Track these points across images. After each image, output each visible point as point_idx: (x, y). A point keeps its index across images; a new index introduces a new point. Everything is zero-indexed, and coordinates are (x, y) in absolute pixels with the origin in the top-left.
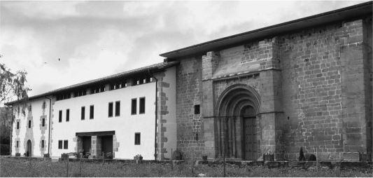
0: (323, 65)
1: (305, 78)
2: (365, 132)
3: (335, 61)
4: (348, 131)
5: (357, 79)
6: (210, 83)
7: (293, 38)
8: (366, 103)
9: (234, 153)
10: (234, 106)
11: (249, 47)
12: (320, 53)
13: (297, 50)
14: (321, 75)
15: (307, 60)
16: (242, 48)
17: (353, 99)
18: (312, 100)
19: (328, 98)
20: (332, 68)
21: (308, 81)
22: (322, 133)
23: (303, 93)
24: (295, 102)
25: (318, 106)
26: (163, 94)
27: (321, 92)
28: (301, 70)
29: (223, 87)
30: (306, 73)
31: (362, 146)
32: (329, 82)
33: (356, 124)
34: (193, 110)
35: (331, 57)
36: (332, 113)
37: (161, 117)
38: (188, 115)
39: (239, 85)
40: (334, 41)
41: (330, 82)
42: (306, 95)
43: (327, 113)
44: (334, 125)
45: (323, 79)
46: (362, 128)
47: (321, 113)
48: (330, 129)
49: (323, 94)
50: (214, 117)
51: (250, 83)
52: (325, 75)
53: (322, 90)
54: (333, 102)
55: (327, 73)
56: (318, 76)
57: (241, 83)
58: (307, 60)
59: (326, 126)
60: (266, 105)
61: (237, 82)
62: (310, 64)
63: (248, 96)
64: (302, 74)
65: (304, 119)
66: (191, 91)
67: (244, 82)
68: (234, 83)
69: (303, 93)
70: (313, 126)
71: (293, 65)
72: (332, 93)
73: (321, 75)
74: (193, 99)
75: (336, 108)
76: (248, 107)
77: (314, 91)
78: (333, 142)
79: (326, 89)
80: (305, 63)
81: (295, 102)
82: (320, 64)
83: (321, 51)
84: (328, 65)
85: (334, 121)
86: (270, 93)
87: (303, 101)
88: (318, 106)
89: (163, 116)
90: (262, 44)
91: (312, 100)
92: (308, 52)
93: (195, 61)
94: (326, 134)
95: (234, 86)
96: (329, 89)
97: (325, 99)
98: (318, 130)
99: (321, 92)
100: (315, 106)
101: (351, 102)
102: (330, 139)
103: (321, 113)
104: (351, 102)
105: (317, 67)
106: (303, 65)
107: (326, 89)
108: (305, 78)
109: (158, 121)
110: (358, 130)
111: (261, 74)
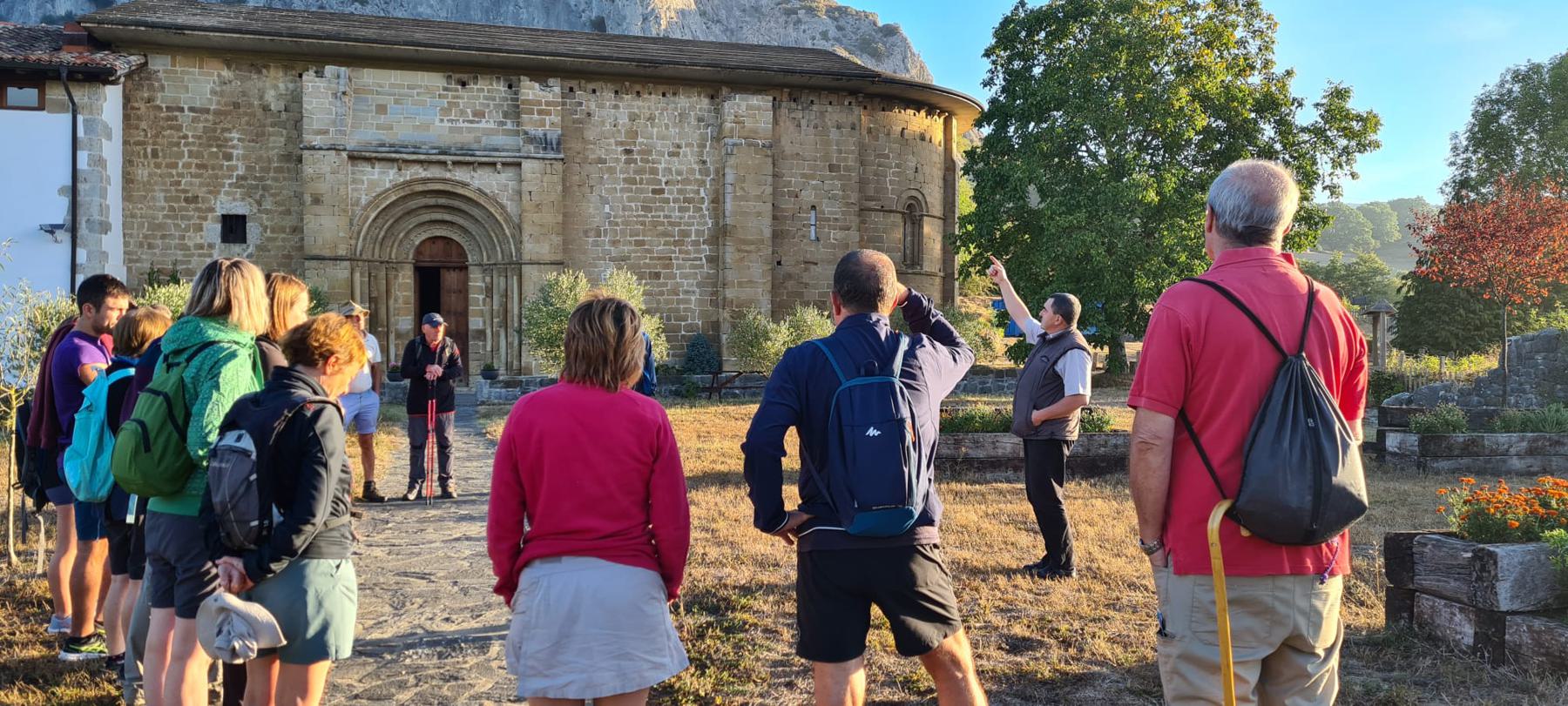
3: (696, 167)
5: (759, 214)
7: (594, 91)
11: (464, 84)
12: (660, 143)
13: (603, 123)
14: (662, 191)
15: (628, 152)
16: (435, 80)
18: (640, 243)
19: (676, 243)
20: (686, 181)
21: (630, 200)
24: (596, 244)
28: (611, 171)
30: (625, 180)
32: (681, 209)
38: (191, 244)
39: (444, 181)
40: (694, 122)
44: (687, 301)
45: (667, 201)
47: (657, 276)
48: (677, 310)
49: (665, 234)
52: (671, 192)
54: (687, 252)
55: (675, 189)
56: (654, 192)
58: (628, 152)
59: (667, 302)
64: (616, 181)
72: (686, 234)
73: (662, 191)
75: (695, 267)
77: (643, 224)
81: (596, 244)
82: (661, 167)
84: (679, 173)
85: (687, 292)
87: (614, 243)
93: (226, 73)
96: (679, 224)
101: (742, 259)
103: (657, 276)
104: (742, 259)
105: (654, 171)
106: (617, 161)
107: (671, 224)
108: (622, 190)
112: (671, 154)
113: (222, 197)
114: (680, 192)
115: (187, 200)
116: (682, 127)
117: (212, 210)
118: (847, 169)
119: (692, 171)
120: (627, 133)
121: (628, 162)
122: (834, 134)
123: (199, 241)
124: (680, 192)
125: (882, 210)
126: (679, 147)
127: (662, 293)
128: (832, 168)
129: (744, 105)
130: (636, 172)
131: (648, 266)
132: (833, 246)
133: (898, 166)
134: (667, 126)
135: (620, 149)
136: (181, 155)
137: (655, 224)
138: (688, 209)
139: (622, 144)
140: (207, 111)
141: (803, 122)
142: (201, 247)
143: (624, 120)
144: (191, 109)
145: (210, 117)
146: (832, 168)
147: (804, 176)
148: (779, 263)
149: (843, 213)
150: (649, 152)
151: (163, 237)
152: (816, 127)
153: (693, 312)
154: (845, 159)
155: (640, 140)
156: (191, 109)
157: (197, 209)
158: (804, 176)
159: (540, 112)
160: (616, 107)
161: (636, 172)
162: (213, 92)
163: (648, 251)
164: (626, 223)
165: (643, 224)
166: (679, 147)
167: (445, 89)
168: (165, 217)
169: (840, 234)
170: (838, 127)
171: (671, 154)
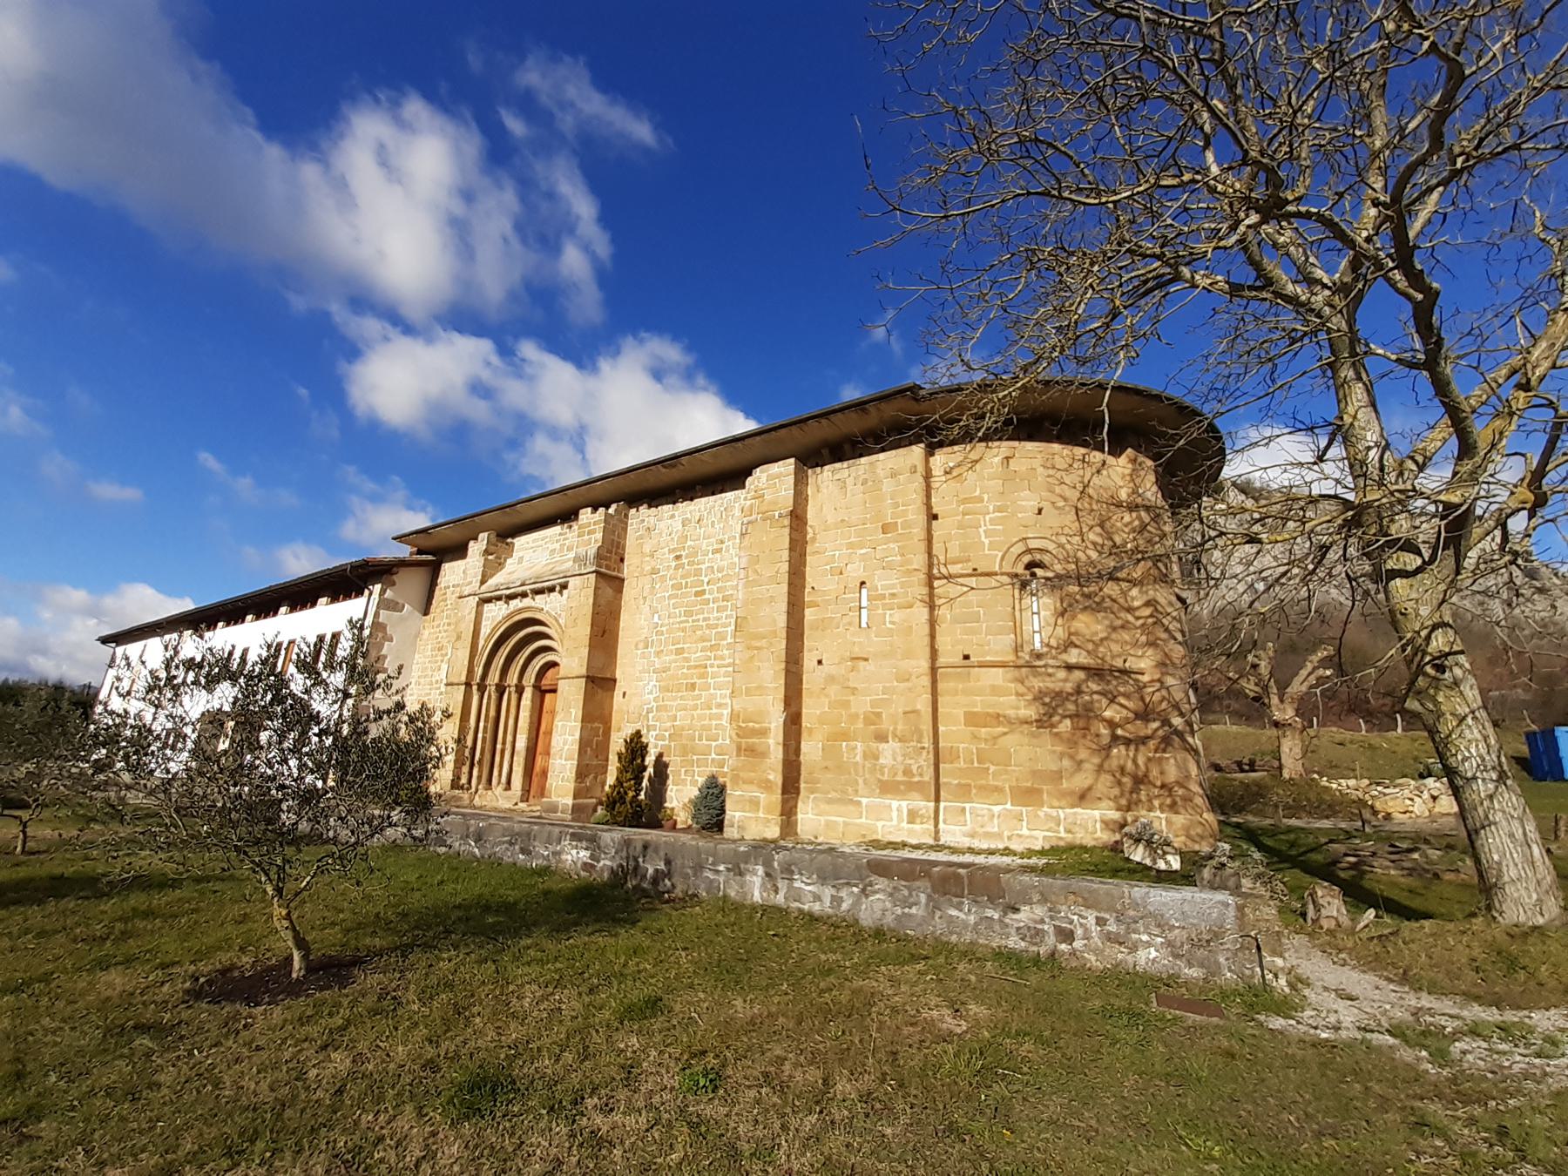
2: (781, 739)
4: (742, 733)
6: (474, 601)
8: (787, 662)
9: (504, 779)
14: (703, 592)
17: (757, 648)
18: (680, 652)
20: (727, 578)
29: (496, 614)
31: (771, 777)
36: (718, 687)
39: (528, 609)
46: (773, 726)
47: (693, 687)
51: (548, 606)
54: (722, 658)
56: (697, 594)
58: (678, 557)
59: (701, 718)
60: (572, 658)
61: (527, 602)
63: (548, 637)
68: (521, 605)
73: (703, 592)
77: (684, 630)
85: (719, 706)
86: (584, 630)
91: (680, 652)
95: (520, 611)
103: (693, 687)
105: (698, 573)
110: (764, 733)
111: (572, 582)
118: (906, 525)
121: (676, 568)
122: (888, 486)
124: (719, 590)
125: (975, 573)
127: (695, 708)
128: (885, 529)
130: (683, 577)
131: (686, 676)
132: (890, 632)
133: (999, 509)
139: (674, 550)
141: (850, 481)
146: (885, 529)
147: (850, 546)
148: (820, 662)
149: (903, 585)
158: (850, 546)
160: (673, 516)
161: (683, 577)
163: (687, 660)
165: (684, 630)
169: (898, 615)
170: (893, 475)
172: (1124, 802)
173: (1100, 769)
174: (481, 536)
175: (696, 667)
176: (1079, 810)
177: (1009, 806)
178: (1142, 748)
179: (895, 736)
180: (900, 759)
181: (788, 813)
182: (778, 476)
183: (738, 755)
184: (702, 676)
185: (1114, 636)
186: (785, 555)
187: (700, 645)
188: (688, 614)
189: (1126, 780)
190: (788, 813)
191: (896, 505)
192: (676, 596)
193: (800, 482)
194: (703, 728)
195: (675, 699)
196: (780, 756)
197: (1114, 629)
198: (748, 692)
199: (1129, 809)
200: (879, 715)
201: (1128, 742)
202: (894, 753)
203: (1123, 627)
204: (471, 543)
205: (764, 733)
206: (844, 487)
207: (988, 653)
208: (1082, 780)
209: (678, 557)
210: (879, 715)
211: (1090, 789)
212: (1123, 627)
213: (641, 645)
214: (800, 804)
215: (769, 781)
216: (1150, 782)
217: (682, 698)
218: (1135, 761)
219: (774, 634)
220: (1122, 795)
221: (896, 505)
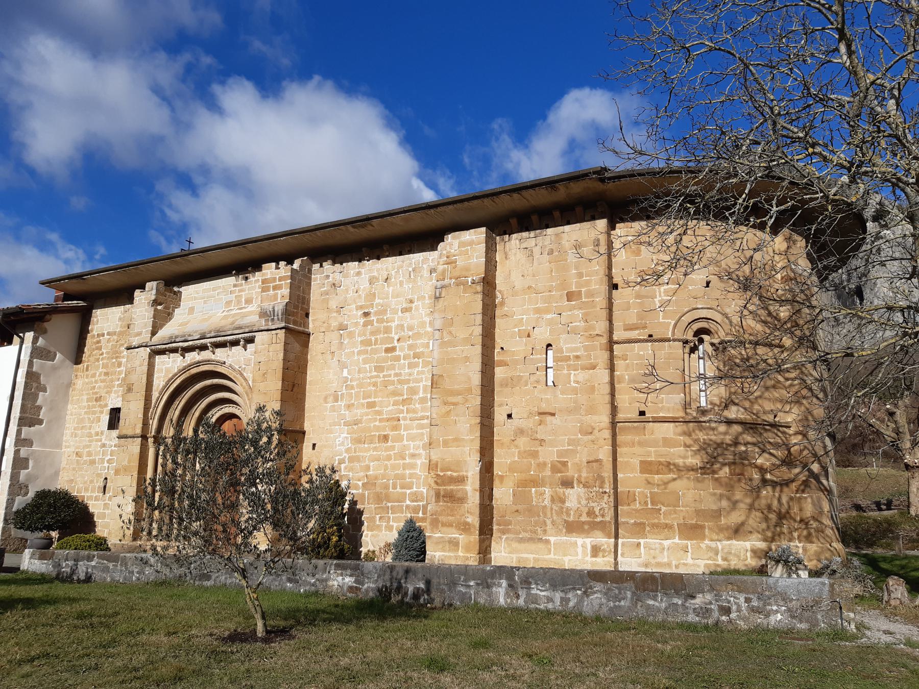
0: (401, 327)
1: (359, 353)
2: (477, 486)
4: (440, 481)
5: (467, 359)
6: (145, 352)
8: (482, 417)
10: (197, 414)
13: (347, 290)
14: (393, 349)
18: (371, 405)
20: (418, 335)
21: (365, 361)
22: (386, 487)
23: (352, 387)
24: (333, 409)
25: (381, 420)
26: (31, 376)
27: (390, 388)
28: (351, 335)
29: (169, 367)
31: (469, 520)
32: (411, 366)
33: (459, 465)
34: (106, 418)
35: (417, 309)
36: (412, 438)
37: (19, 432)
38: (93, 432)
39: (208, 362)
41: (411, 366)
42: (357, 394)
43: (400, 439)
45: (398, 358)
46: (470, 474)
47: (385, 438)
49: (395, 393)
50: (142, 436)
51: (231, 359)
52: (402, 350)
53: (393, 383)
54: (414, 411)
55: (405, 344)
56: (388, 350)
57: (213, 357)
58: (366, 314)
59: (394, 467)
61: (206, 355)
62: (371, 323)
65: (347, 451)
66: (107, 374)
67: (220, 354)
69: (352, 387)
70: (368, 468)
71: (334, 324)
72: (413, 391)
73: (393, 349)
74: (108, 393)
76: (232, 416)
77: (375, 384)
78: (407, 507)
79: (400, 382)
80: (362, 321)
82: (393, 325)
83: (398, 296)
84: (411, 328)
85: (413, 456)
87: (349, 407)
88: (381, 420)
89: (25, 429)
90: (269, 269)
91: (371, 405)
92: (371, 296)
94: (395, 487)
95: (198, 364)
97: (395, 403)
98: (376, 478)
99: (390, 388)
100: (375, 420)
101: (448, 413)
102: (401, 499)
103: (385, 438)
104: (448, 413)
105: (387, 330)
106: (357, 324)
107: (400, 382)
108: (359, 353)
109: (8, 439)
110: (461, 480)
111: (259, 337)
112: (405, 310)
113: (113, 395)
114: (411, 347)
115: (96, 400)
116: (415, 281)
117: (106, 405)
118: (590, 294)
119: (423, 324)
120: (367, 295)
121: (365, 325)
123: (98, 430)
124: (411, 347)
126: (411, 302)
127: (389, 458)
128: (570, 296)
129: (456, 243)
130: (373, 333)
131: (377, 428)
132: (575, 391)
134: (401, 283)
135: (360, 313)
136: (97, 368)
137: (386, 384)
138: (416, 365)
139: (361, 307)
140: (114, 333)
141: (537, 251)
142: (97, 434)
143: (364, 285)
144: (108, 334)
145: (115, 337)
146: (570, 296)
147: (538, 311)
148: (510, 416)
149: (586, 348)
150: (384, 312)
151: (83, 428)
152: (551, 252)
153: (418, 478)
154: (588, 283)
155: (377, 301)
156: (108, 334)
157: (100, 406)
158: (538, 311)
159: (275, 288)
160: (359, 274)
161: (373, 333)
162: (120, 319)
163: (379, 413)
164: (361, 386)
165: (375, 384)
166: (411, 302)
167: (235, 286)
168: (86, 413)
169: (582, 375)
171: (405, 310)
172: (769, 534)
173: (751, 507)
174: (149, 285)
175: (388, 420)
176: (734, 542)
177: (677, 540)
178: (785, 489)
179: (579, 482)
180: (584, 502)
181: (484, 551)
182: (471, 243)
183: (437, 501)
184: (395, 428)
185: (766, 394)
186: (479, 318)
187: (392, 399)
188: (379, 369)
189: (773, 517)
190: (484, 551)
191: (580, 275)
192: (366, 352)
193: (491, 249)
194: (397, 477)
195: (368, 450)
196: (477, 501)
197: (767, 388)
198: (446, 443)
199: (773, 540)
200: (565, 464)
201: (774, 484)
202: (579, 497)
203: (774, 387)
204: (137, 293)
205: (461, 480)
206: (531, 255)
207: (662, 409)
208: (736, 517)
209: (366, 314)
210: (565, 464)
211: (743, 524)
212: (774, 387)
213: (331, 399)
214: (493, 543)
215: (468, 524)
216: (791, 518)
217: (375, 449)
218: (779, 500)
219: (469, 390)
220: (768, 527)
221: (580, 275)
